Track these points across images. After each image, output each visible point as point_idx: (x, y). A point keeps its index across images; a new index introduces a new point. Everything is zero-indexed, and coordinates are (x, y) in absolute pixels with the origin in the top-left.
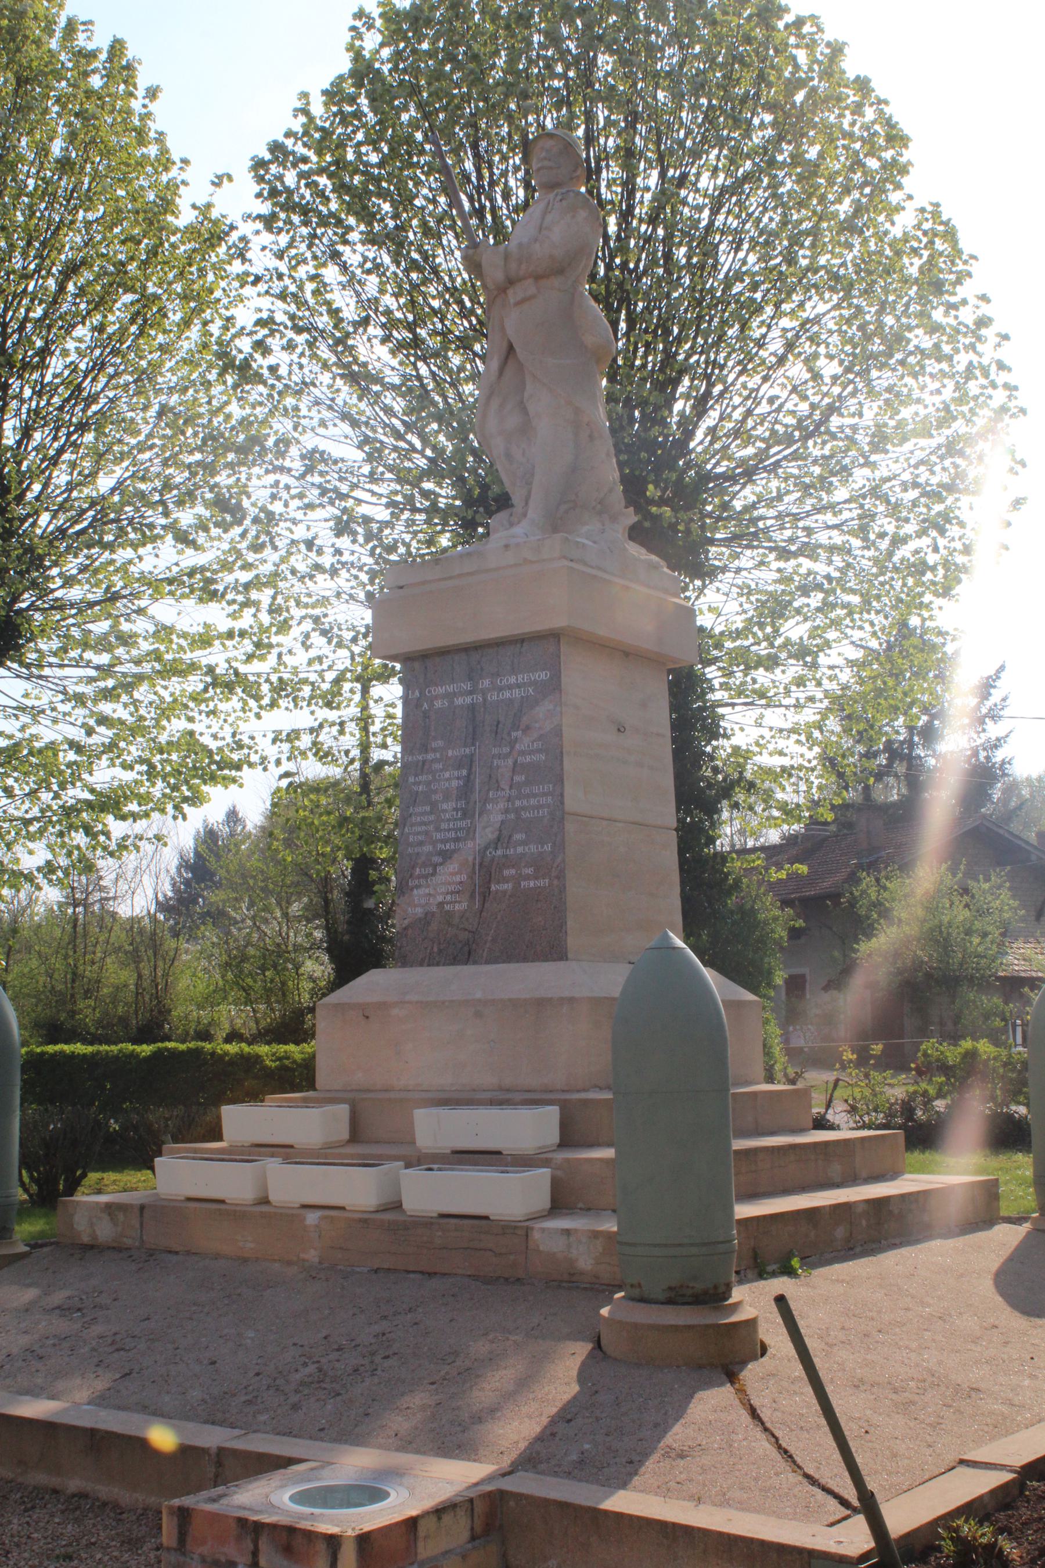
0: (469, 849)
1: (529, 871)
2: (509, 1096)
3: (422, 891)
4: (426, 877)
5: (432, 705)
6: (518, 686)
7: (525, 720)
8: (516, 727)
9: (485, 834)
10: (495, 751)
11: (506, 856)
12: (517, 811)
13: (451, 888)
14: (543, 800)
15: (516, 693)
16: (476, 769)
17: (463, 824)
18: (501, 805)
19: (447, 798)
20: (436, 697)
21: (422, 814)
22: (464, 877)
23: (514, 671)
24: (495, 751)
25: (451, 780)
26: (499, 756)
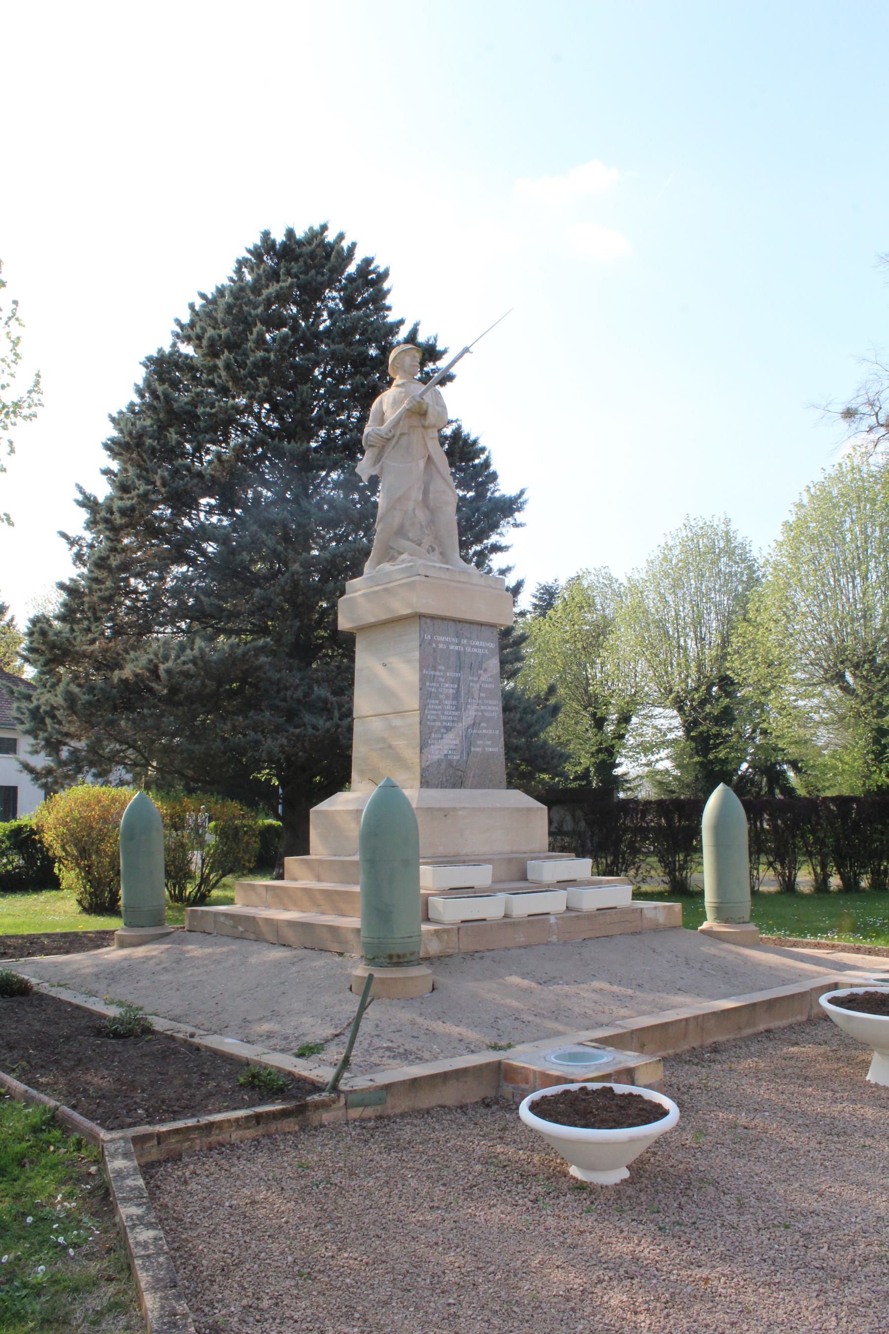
0: (461, 726)
1: (489, 743)
2: (533, 855)
3: (436, 747)
4: (438, 739)
5: (437, 646)
6: (481, 647)
7: (484, 666)
8: (480, 668)
9: (467, 721)
10: (470, 678)
11: (478, 734)
12: (482, 711)
13: (451, 747)
14: (494, 708)
15: (480, 651)
16: (461, 683)
17: (456, 713)
18: (474, 707)
19: (447, 698)
20: (440, 642)
21: (436, 704)
22: (457, 742)
23: (479, 639)
24: (470, 678)
25: (449, 689)
26: (473, 681)
